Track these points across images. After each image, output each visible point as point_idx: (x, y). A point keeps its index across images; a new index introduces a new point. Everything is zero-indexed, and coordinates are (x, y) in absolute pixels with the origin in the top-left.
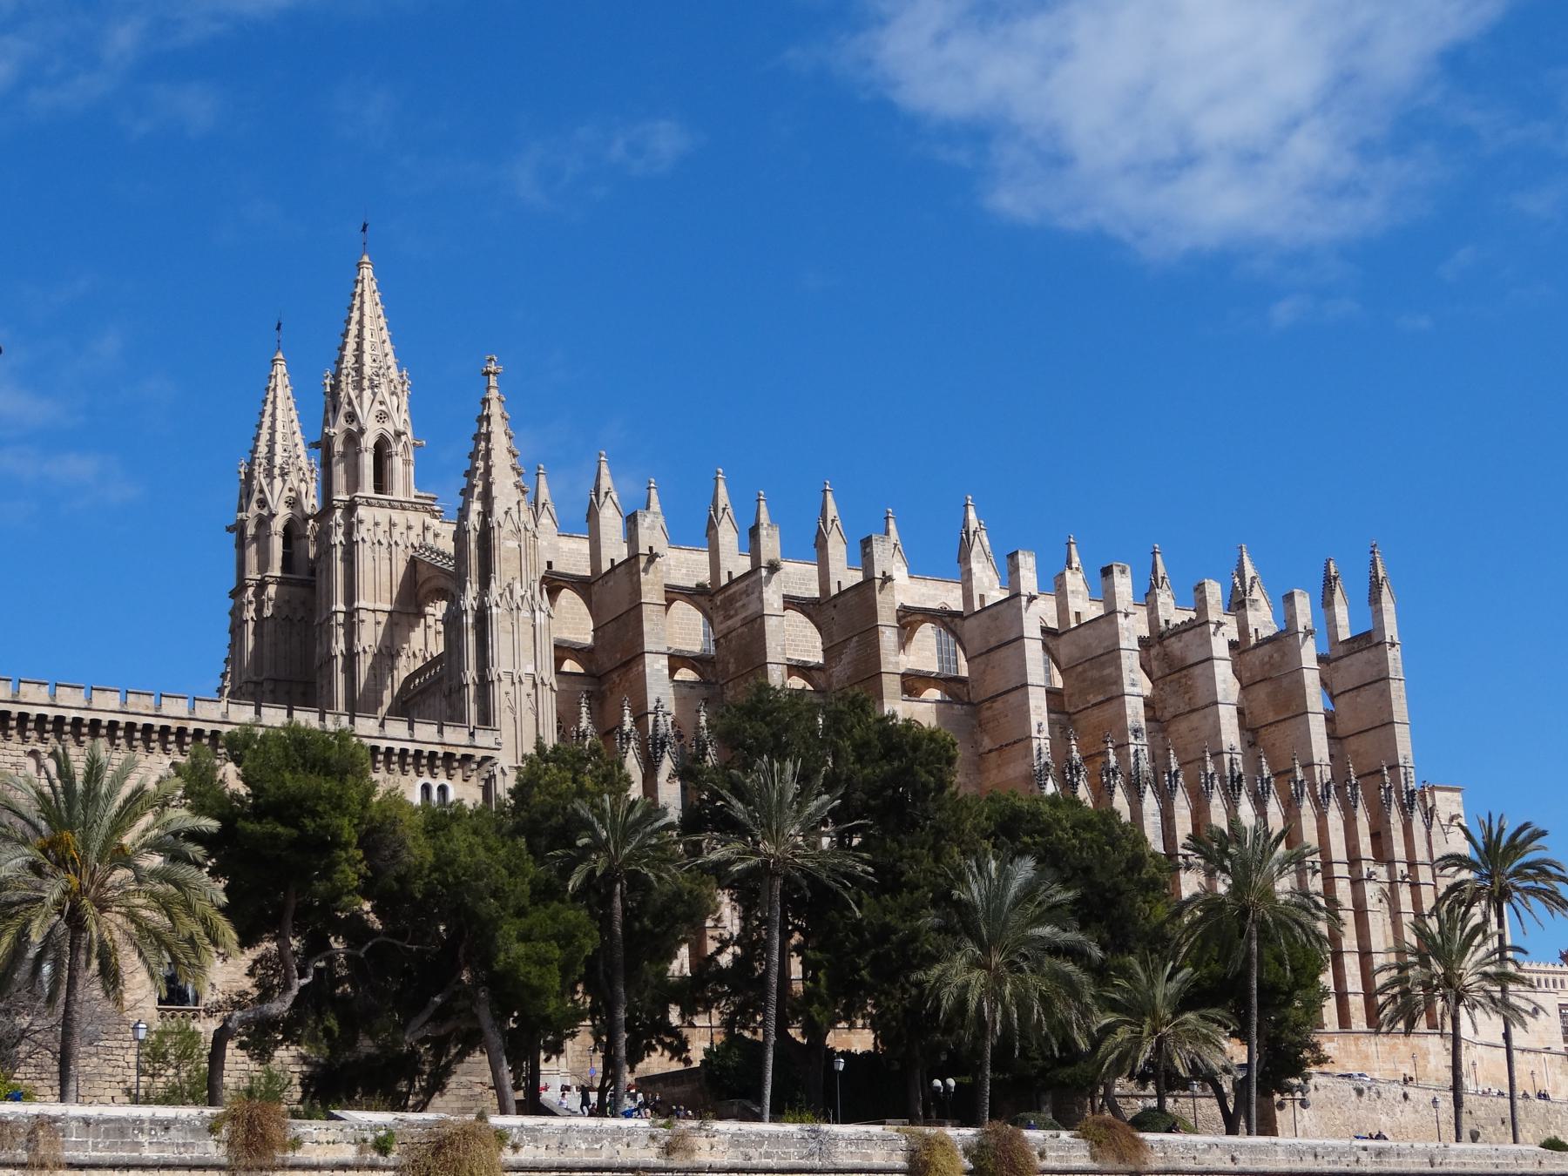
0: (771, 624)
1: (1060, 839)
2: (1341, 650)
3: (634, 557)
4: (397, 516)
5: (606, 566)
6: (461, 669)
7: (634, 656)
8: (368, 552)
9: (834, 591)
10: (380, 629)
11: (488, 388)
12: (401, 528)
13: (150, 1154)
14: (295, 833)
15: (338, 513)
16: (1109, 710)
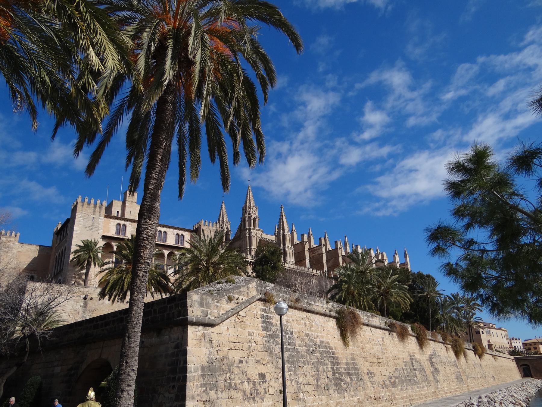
4: (257, 232)
11: (282, 210)
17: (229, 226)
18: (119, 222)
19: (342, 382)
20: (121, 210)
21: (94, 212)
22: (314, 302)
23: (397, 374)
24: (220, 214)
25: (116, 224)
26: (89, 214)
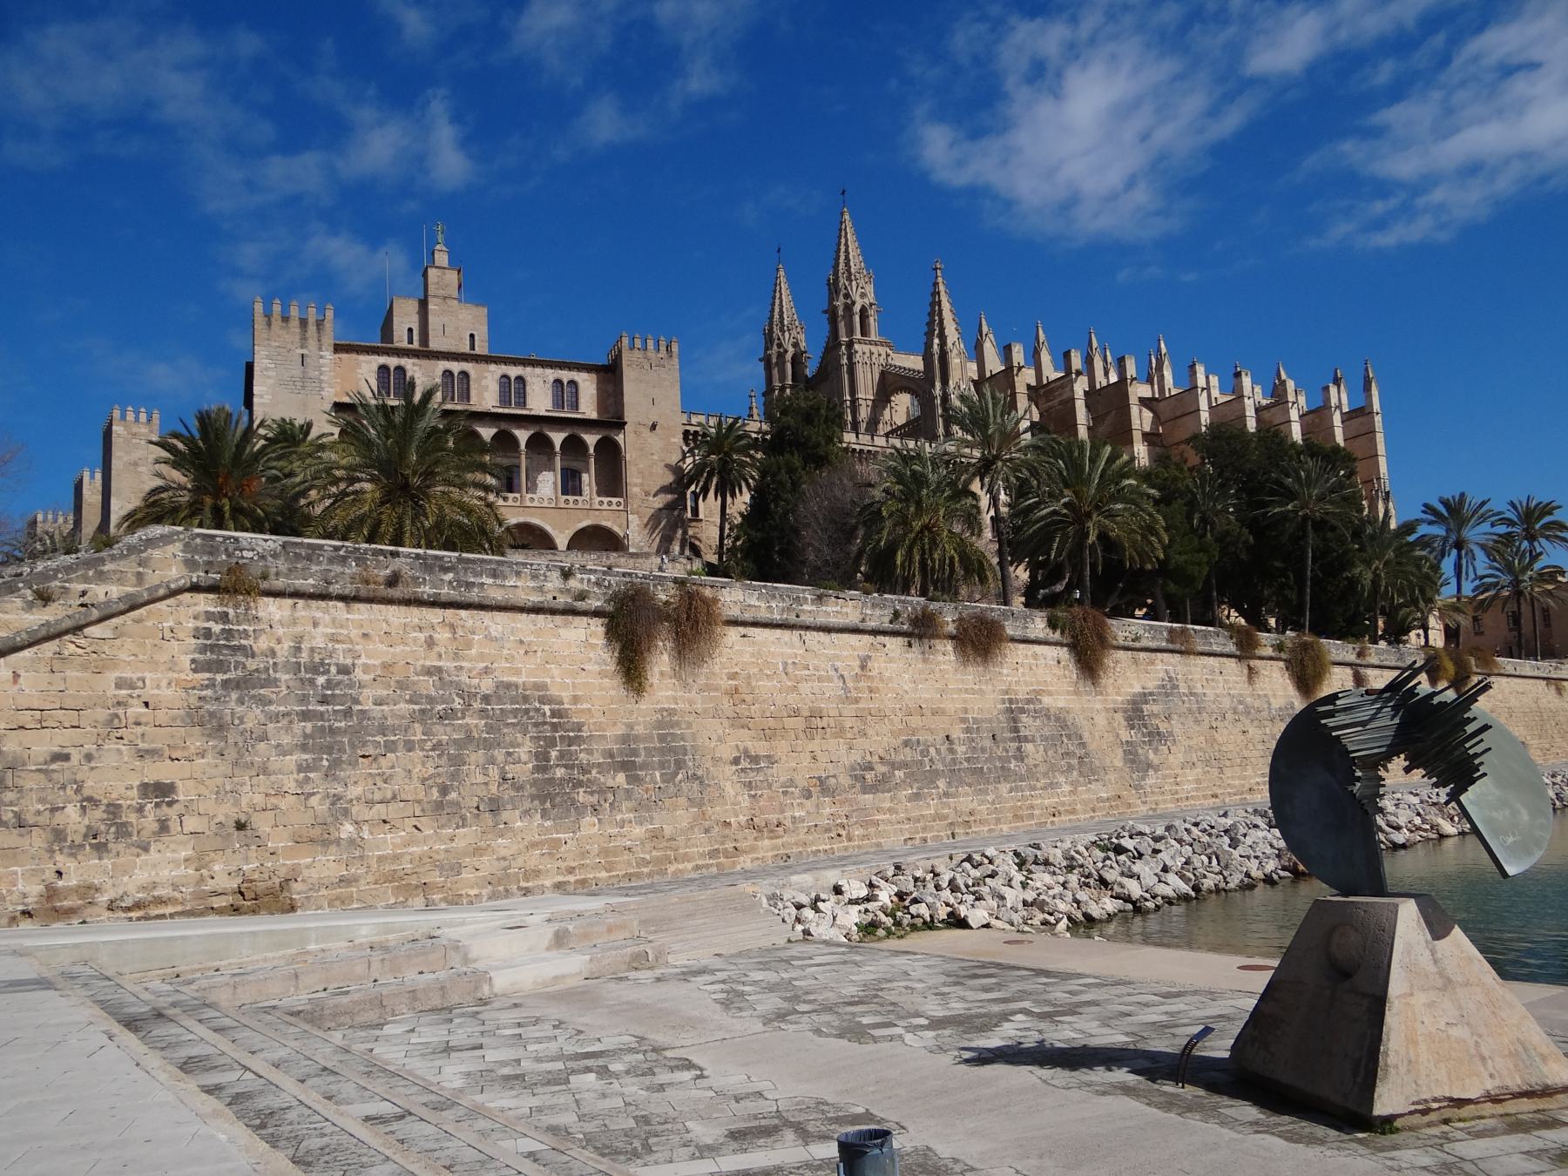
4: (873, 349)
9: (1098, 387)
10: (869, 409)
11: (937, 277)
12: (876, 355)
13: (1215, 648)
15: (843, 347)
17: (802, 337)
18: (383, 360)
19: (581, 790)
20: (417, 324)
21: (304, 339)
22: (494, 575)
23: (907, 755)
24: (773, 304)
25: (375, 368)
26: (289, 346)
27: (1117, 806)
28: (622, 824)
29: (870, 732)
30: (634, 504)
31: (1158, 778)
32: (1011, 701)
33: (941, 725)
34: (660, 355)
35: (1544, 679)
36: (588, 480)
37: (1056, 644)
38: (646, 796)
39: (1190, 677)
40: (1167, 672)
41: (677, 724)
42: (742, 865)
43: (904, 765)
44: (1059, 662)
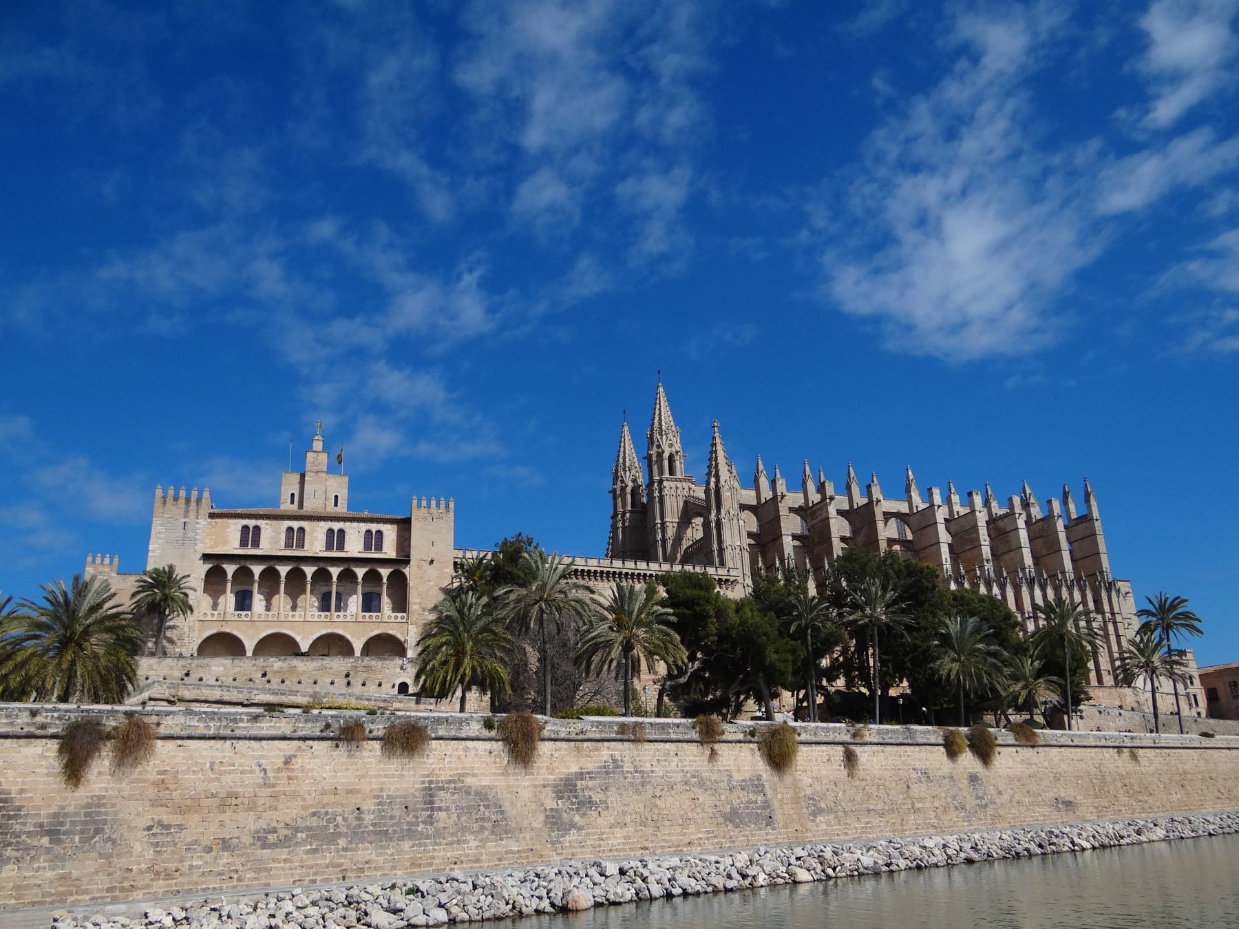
0: (832, 521)
1: (975, 608)
2: (1073, 523)
3: (775, 496)
4: (679, 484)
5: (763, 501)
6: (711, 544)
7: (778, 536)
8: (668, 500)
9: (855, 507)
10: (675, 529)
12: (680, 489)
13: (673, 736)
14: (692, 612)
15: (656, 484)
16: (975, 552)
19: (9, 848)
21: (187, 511)
23: (314, 822)
27: (527, 857)
28: (38, 869)
29: (280, 806)
30: (413, 617)
31: (580, 836)
32: (431, 782)
33: (355, 800)
34: (440, 511)
35: (1114, 747)
36: (386, 602)
37: (490, 739)
38: (63, 852)
39: (638, 759)
40: (612, 755)
41: (104, 805)
42: (134, 897)
43: (309, 829)
44: (490, 753)
